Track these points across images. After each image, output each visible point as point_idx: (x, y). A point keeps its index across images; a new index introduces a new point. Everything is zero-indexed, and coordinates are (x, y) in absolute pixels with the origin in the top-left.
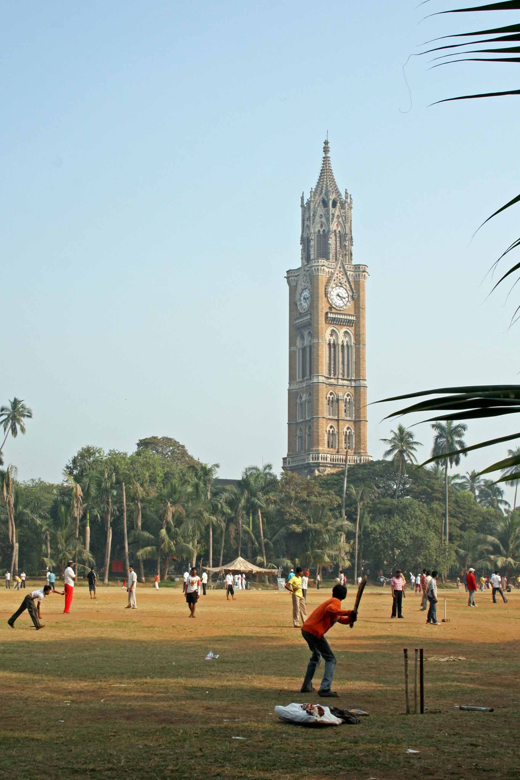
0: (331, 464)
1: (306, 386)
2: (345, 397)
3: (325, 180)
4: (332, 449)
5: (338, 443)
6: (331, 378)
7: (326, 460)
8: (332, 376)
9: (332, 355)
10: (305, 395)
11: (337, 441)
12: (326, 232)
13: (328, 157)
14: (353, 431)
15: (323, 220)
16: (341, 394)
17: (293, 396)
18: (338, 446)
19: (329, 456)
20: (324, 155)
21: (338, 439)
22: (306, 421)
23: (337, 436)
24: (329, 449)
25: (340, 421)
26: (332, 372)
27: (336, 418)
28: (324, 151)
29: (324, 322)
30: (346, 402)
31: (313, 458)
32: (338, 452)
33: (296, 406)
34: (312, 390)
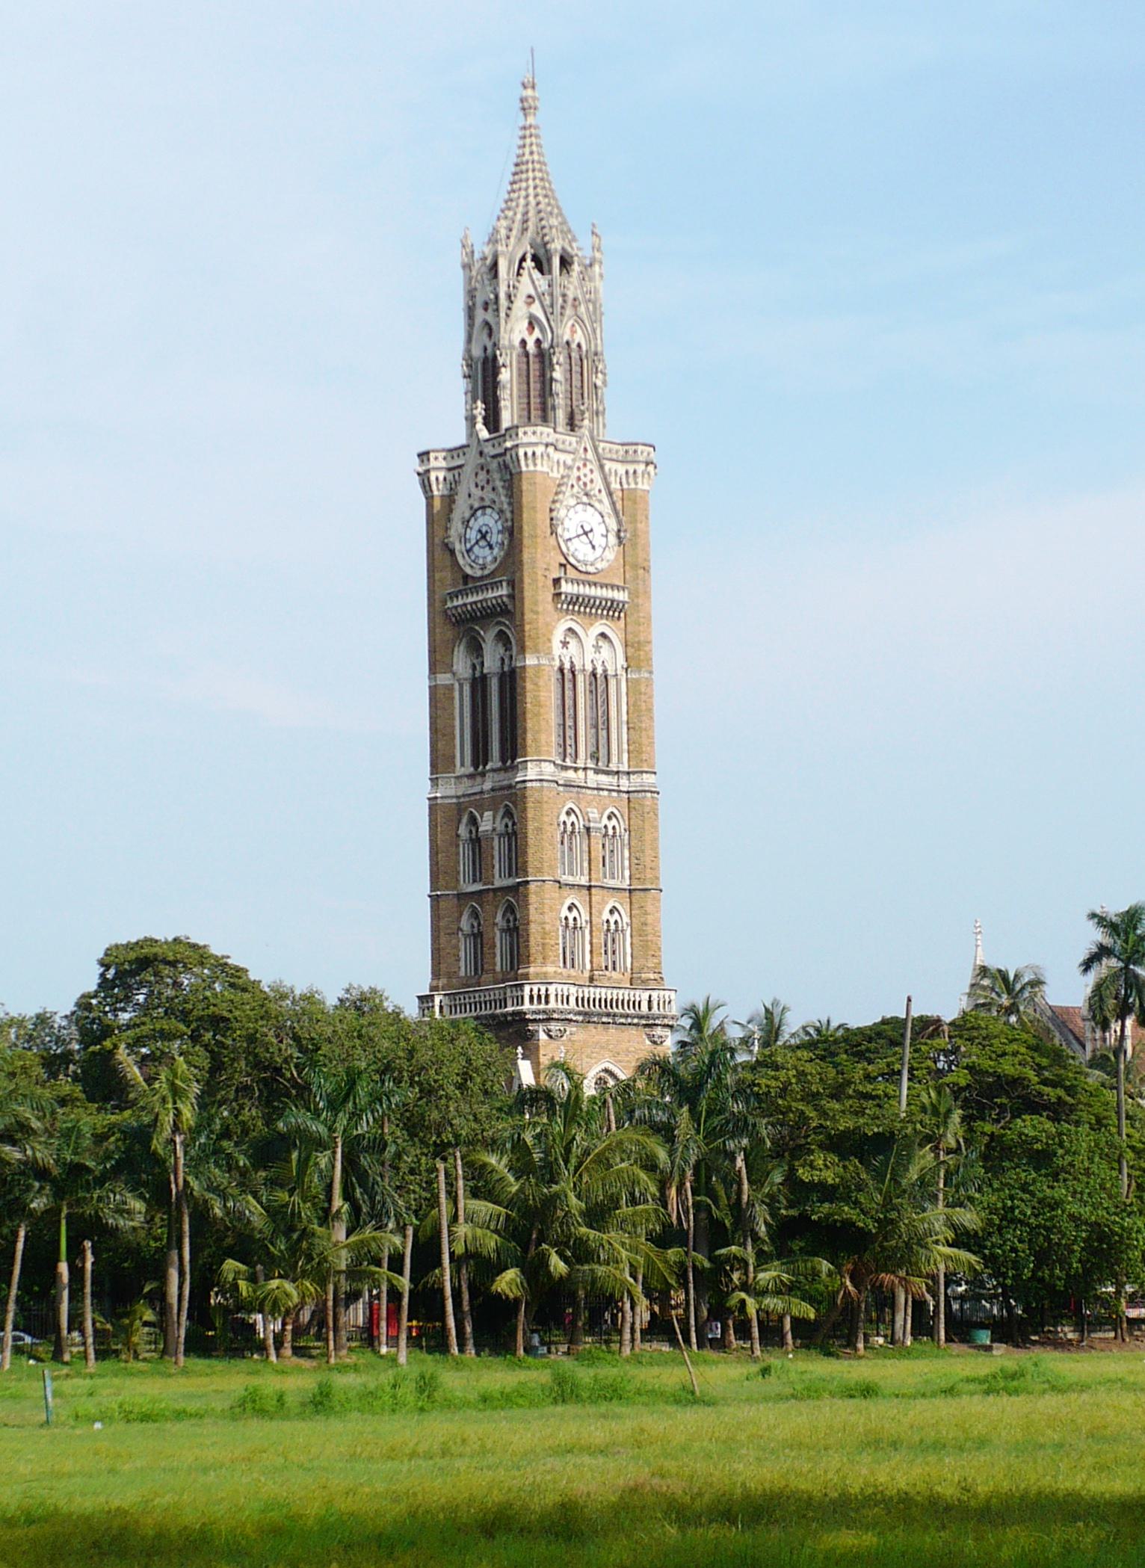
0: (579, 1013)
1: (493, 790)
2: (605, 821)
3: (523, 193)
4: (572, 972)
5: (591, 952)
6: (566, 768)
7: (547, 1002)
8: (569, 763)
9: (569, 702)
10: (488, 814)
11: (588, 947)
12: (545, 345)
13: (536, 127)
14: (626, 919)
15: (537, 310)
16: (594, 814)
17: (445, 819)
18: (591, 962)
19: (573, 989)
20: (521, 122)
21: (591, 944)
22: (494, 890)
23: (587, 932)
24: (564, 971)
25: (593, 890)
26: (569, 750)
27: (584, 881)
28: (524, 109)
29: (550, 607)
30: (606, 835)
31: (531, 997)
32: (591, 979)
33: (458, 846)
34: (512, 803)
